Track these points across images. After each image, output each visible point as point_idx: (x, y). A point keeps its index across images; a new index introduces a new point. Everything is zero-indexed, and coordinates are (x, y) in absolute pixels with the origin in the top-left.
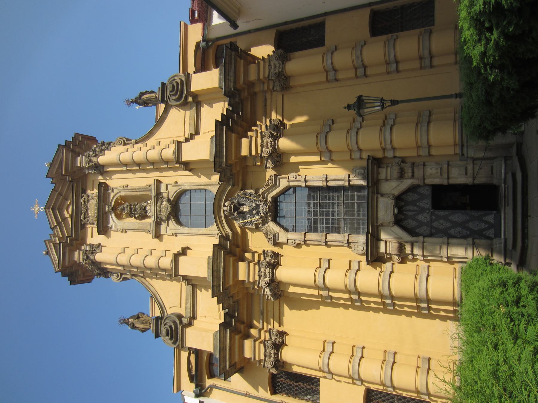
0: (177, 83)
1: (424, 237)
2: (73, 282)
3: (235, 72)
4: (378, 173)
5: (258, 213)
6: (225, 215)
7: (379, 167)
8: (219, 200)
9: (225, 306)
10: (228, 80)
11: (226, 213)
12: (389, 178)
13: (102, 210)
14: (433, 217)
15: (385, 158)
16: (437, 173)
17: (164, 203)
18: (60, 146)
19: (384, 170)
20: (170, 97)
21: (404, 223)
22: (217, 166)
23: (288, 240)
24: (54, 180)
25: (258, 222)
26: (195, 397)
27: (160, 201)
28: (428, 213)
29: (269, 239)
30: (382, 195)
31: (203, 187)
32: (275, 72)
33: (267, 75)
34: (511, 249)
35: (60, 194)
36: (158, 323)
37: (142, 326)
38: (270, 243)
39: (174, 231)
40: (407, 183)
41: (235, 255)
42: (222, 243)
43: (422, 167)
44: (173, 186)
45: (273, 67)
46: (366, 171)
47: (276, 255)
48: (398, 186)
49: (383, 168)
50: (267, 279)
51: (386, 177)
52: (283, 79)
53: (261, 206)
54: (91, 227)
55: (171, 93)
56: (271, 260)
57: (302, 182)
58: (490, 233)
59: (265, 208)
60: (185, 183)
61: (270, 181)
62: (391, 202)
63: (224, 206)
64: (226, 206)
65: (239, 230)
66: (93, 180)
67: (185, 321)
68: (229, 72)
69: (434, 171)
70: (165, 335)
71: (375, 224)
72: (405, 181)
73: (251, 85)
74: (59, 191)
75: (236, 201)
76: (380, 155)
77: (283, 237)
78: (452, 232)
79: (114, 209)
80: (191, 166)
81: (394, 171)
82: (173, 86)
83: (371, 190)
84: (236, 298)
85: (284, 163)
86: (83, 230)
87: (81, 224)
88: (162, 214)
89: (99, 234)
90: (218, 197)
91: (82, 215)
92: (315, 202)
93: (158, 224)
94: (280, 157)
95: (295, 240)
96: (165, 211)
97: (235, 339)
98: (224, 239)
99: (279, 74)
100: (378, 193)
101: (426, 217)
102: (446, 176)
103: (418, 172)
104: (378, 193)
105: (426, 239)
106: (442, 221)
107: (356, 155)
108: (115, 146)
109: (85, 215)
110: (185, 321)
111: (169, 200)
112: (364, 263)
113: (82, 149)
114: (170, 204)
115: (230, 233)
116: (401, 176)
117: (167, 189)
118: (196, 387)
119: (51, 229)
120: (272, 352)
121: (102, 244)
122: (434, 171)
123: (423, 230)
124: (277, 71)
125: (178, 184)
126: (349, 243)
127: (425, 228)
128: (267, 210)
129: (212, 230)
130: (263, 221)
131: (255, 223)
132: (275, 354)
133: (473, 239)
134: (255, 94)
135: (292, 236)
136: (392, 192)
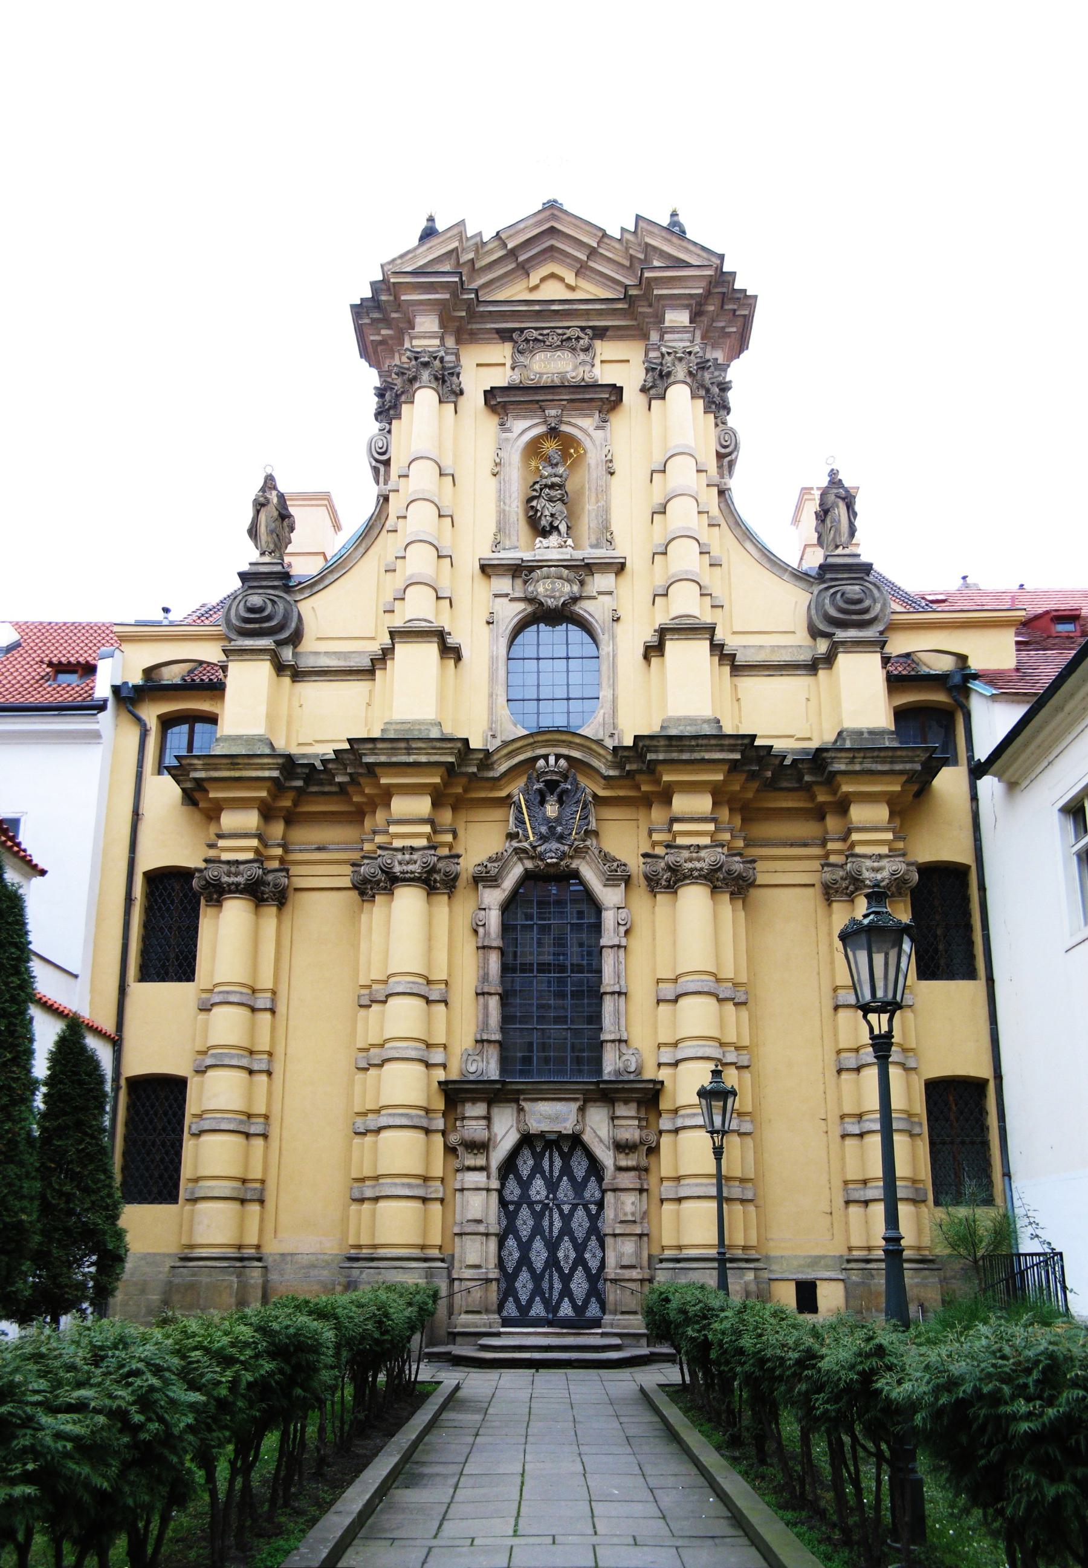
0: (866, 611)
1: (500, 1192)
2: (358, 311)
3: (871, 772)
4: (626, 1102)
5: (544, 839)
6: (536, 759)
7: (640, 1103)
9: (330, 766)
10: (854, 757)
12: (616, 1122)
14: (538, 1208)
15: (659, 1114)
16: (625, 1214)
17: (567, 588)
18: (722, 257)
19: (633, 1113)
20: (832, 591)
21: (526, 1153)
25: (523, 839)
26: (113, 686)
27: (572, 575)
28: (547, 1197)
30: (582, 1110)
32: (864, 871)
33: (859, 850)
34: (480, 1342)
35: (593, 252)
36: (276, 579)
40: (606, 1157)
41: (446, 784)
43: (638, 1186)
45: (876, 864)
46: (632, 1077)
47: (450, 884)
48: (601, 1141)
49: (638, 1110)
50: (397, 869)
51: (618, 1118)
52: (847, 888)
53: (559, 845)
55: (839, 595)
58: (511, 1310)
61: (615, 864)
62: (567, 1127)
63: (558, 757)
64: (556, 761)
65: (503, 794)
66: (628, 361)
67: (287, 654)
68: (872, 757)
69: (629, 1208)
70: (249, 604)
71: (522, 1097)
72: (611, 1153)
73: (842, 807)
74: (601, 251)
76: (665, 1104)
78: (511, 1242)
79: (553, 432)
80: (654, 661)
81: (630, 1132)
82: (860, 601)
83: (592, 1087)
84: (350, 789)
86: (496, 336)
87: (514, 330)
88: (541, 582)
89: (485, 392)
91: (535, 334)
93: (516, 570)
94: (668, 887)
96: (547, 590)
97: (259, 789)
99: (858, 880)
100: (586, 1101)
101: (538, 1193)
102: (617, 1231)
103: (627, 1180)
104: (586, 1101)
105: (494, 1196)
106: (531, 1223)
107: (667, 1056)
109: (536, 340)
110: (287, 654)
111: (575, 599)
112: (440, 1075)
113: (713, 321)
114: (564, 604)
115: (496, 774)
116: (621, 1147)
117: (600, 593)
118: (136, 687)
119: (498, 233)
120: (240, 879)
121: (462, 400)
122: (629, 1208)
123: (513, 1191)
124: (866, 874)
126: (482, 1041)
127: (517, 1192)
130: (524, 851)
131: (520, 832)
132: (238, 884)
133: (497, 1280)
135: (494, 918)
136: (588, 1129)
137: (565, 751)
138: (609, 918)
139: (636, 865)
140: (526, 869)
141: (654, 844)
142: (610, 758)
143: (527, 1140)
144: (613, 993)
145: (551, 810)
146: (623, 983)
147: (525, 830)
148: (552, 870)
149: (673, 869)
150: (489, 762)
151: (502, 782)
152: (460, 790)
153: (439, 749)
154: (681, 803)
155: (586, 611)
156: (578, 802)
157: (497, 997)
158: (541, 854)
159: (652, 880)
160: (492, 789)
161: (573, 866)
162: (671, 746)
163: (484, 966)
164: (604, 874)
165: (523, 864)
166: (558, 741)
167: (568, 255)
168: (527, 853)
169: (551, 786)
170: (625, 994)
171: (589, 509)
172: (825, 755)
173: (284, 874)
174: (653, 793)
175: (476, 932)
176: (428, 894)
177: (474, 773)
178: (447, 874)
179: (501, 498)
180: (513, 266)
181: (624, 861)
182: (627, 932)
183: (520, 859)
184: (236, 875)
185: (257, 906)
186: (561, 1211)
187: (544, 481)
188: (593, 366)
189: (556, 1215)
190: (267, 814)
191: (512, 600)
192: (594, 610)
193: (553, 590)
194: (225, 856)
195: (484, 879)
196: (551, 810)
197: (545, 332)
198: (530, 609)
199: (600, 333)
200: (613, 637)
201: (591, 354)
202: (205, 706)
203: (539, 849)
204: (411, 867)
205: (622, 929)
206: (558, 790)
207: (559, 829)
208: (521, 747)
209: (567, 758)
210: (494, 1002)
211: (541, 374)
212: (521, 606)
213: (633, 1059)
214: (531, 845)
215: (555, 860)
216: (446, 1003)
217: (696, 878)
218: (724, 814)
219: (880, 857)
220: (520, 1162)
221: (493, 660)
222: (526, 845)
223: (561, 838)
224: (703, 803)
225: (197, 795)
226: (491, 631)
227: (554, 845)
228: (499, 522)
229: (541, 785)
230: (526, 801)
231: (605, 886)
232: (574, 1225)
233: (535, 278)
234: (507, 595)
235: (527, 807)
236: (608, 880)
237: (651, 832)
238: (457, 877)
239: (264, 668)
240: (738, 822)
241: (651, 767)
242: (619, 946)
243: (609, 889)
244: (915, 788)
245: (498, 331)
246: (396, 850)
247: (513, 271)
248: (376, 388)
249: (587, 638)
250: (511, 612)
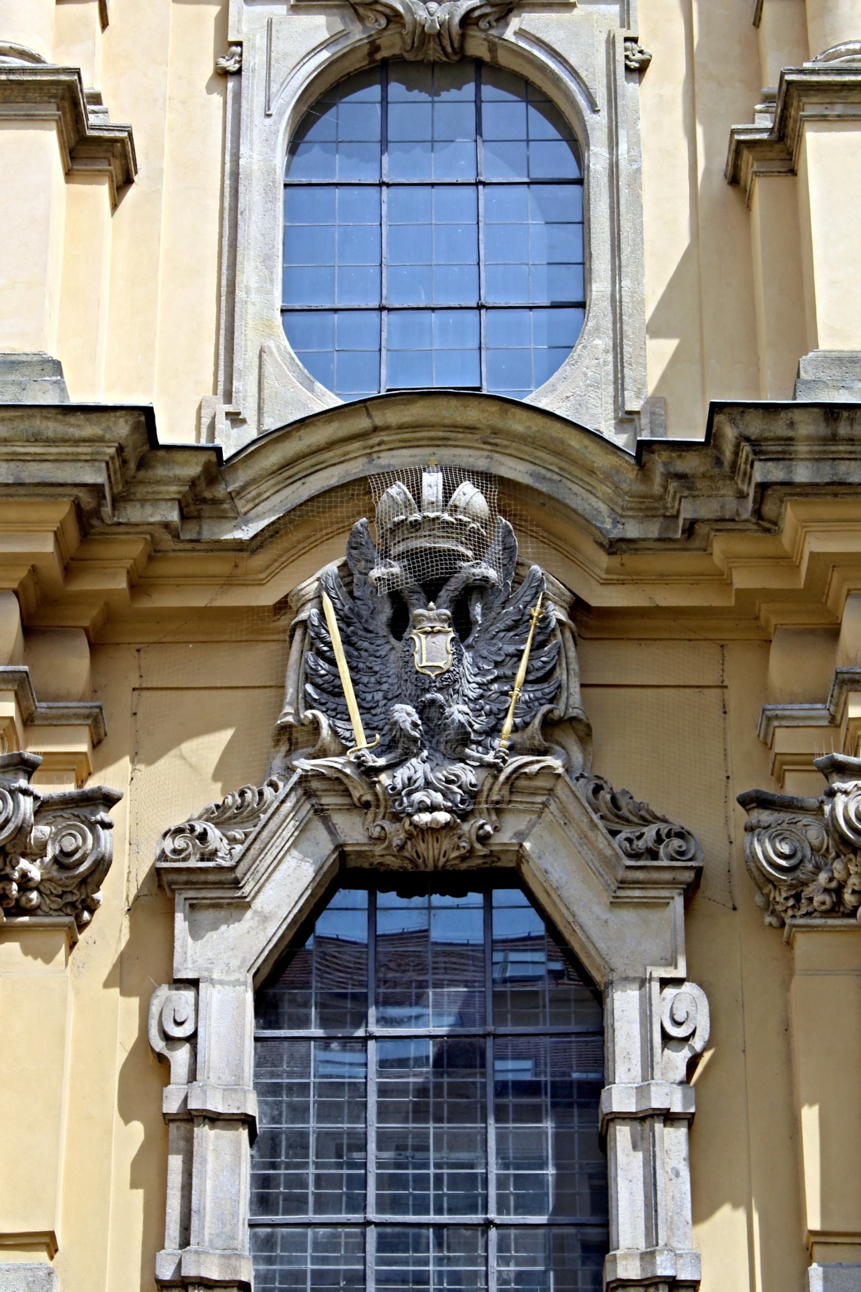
8: (496, 432)
11: (398, 490)
22: (755, 426)
23: (194, 983)
29: (203, 837)
31: (600, 287)
38: (169, 845)
39: (254, 60)
42: (161, 472)
44: (611, 42)
56: (36, 853)
57: (642, 1091)
59: (438, 798)
60: (635, 142)
61: (650, 832)
64: (449, 492)
65: (268, 597)
75: (492, 574)
85: (789, 943)
90: (519, 423)
92: (492, 1192)
95: (192, 1038)
98: (193, 483)
114: (467, 20)
115: (245, 533)
125: (628, 88)
128: (424, 818)
129: (269, 368)
130: (337, 781)
137: (479, 461)
140: (340, 848)
142: (630, 473)
150: (221, 491)
151: (260, 560)
153: (49, 442)
155: (539, 42)
156: (518, 624)
158: (396, 793)
159: (774, 884)
160: (230, 582)
161: (505, 837)
162: (834, 439)
164: (605, 861)
165: (332, 831)
166: (455, 427)
168: (347, 793)
174: (768, 595)
177: (166, 526)
181: (678, 822)
203: (384, 779)
206: (454, 585)
208: (330, 446)
215: (443, 817)
230: (342, 619)
231: (616, 903)
235: (347, 641)
236: (623, 884)
241: (769, 509)
243: (629, 916)
249: (544, 127)
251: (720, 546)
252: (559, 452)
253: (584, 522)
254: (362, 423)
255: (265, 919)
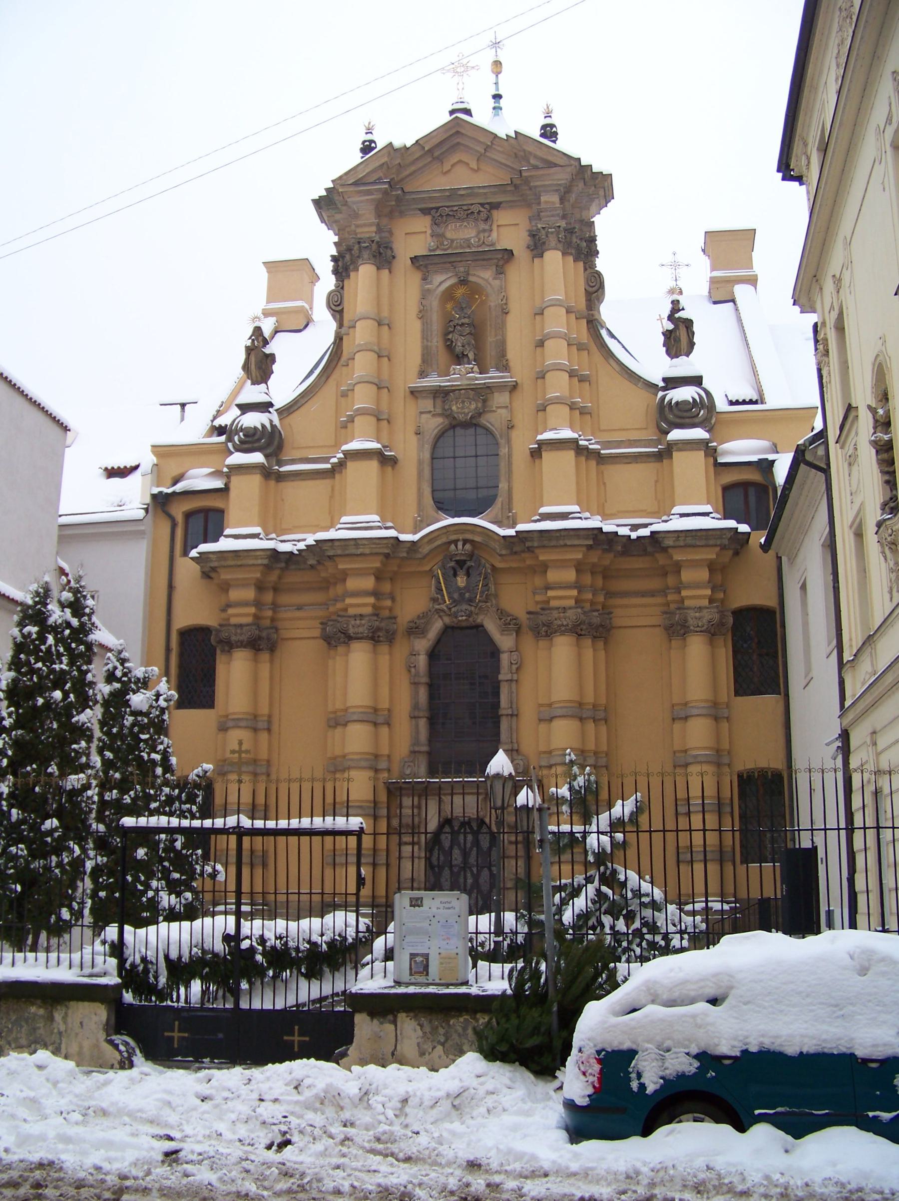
6: (450, 543)
11: (453, 547)
13: (459, 259)
24: (513, 141)
32: (690, 619)
33: (687, 603)
37: (253, 367)
50: (351, 631)
54: (424, 230)
64: (464, 545)
73: (677, 568)
77: (422, 645)
79: (463, 282)
94: (547, 635)
108: (585, 269)
114: (471, 418)
115: (420, 556)
126: (414, 752)
130: (443, 611)
132: (242, 642)
134: (665, 574)
135: (422, 661)
138: (505, 658)
139: (523, 616)
140: (444, 624)
141: (537, 603)
143: (446, 822)
144: (507, 715)
145: (461, 581)
146: (514, 706)
147: (443, 596)
148: (464, 624)
149: (548, 625)
152: (395, 569)
154: (553, 576)
156: (480, 574)
157: (425, 719)
161: (479, 621)
163: (415, 696)
167: (471, 149)
169: (461, 563)
170: (517, 715)
171: (491, 339)
172: (657, 536)
173: (274, 631)
175: (409, 671)
176: (374, 646)
178: (387, 631)
179: (425, 335)
180: (430, 159)
182: (517, 669)
183: (440, 617)
184: (241, 634)
185: (256, 654)
186: (472, 871)
187: (456, 322)
188: (491, 230)
189: (469, 875)
190: (260, 587)
191: (434, 415)
192: (495, 419)
193: (463, 408)
194: (234, 621)
195: (416, 630)
196: (461, 581)
197: (455, 208)
198: (447, 422)
199: (496, 206)
200: (509, 441)
201: (489, 223)
202: (218, 503)
204: (361, 630)
205: (514, 667)
206: (466, 566)
207: (467, 595)
209: (472, 542)
210: (423, 723)
211: (452, 241)
212: (440, 420)
213: (521, 763)
214: (447, 606)
215: (464, 618)
216: (389, 725)
217: (564, 631)
218: (587, 579)
219: (700, 609)
220: (443, 837)
221: (420, 462)
222: (443, 607)
223: (470, 601)
224: (570, 575)
225: (213, 575)
226: (419, 440)
227: (464, 607)
228: (423, 355)
229: (453, 564)
230: (443, 574)
232: (481, 881)
233: (447, 167)
234: (430, 412)
235: (444, 578)
237: (534, 593)
238: (394, 633)
239: (256, 479)
240: (600, 582)
242: (511, 680)
243: (505, 637)
244: (731, 552)
245: (420, 210)
246: (350, 617)
247: (430, 162)
248: (332, 256)
250: (433, 424)
251: (523, 555)
252: (488, 535)
253: (494, 550)
254: (445, 531)
255: (429, 640)
